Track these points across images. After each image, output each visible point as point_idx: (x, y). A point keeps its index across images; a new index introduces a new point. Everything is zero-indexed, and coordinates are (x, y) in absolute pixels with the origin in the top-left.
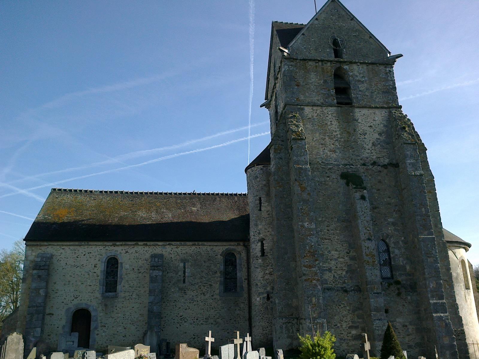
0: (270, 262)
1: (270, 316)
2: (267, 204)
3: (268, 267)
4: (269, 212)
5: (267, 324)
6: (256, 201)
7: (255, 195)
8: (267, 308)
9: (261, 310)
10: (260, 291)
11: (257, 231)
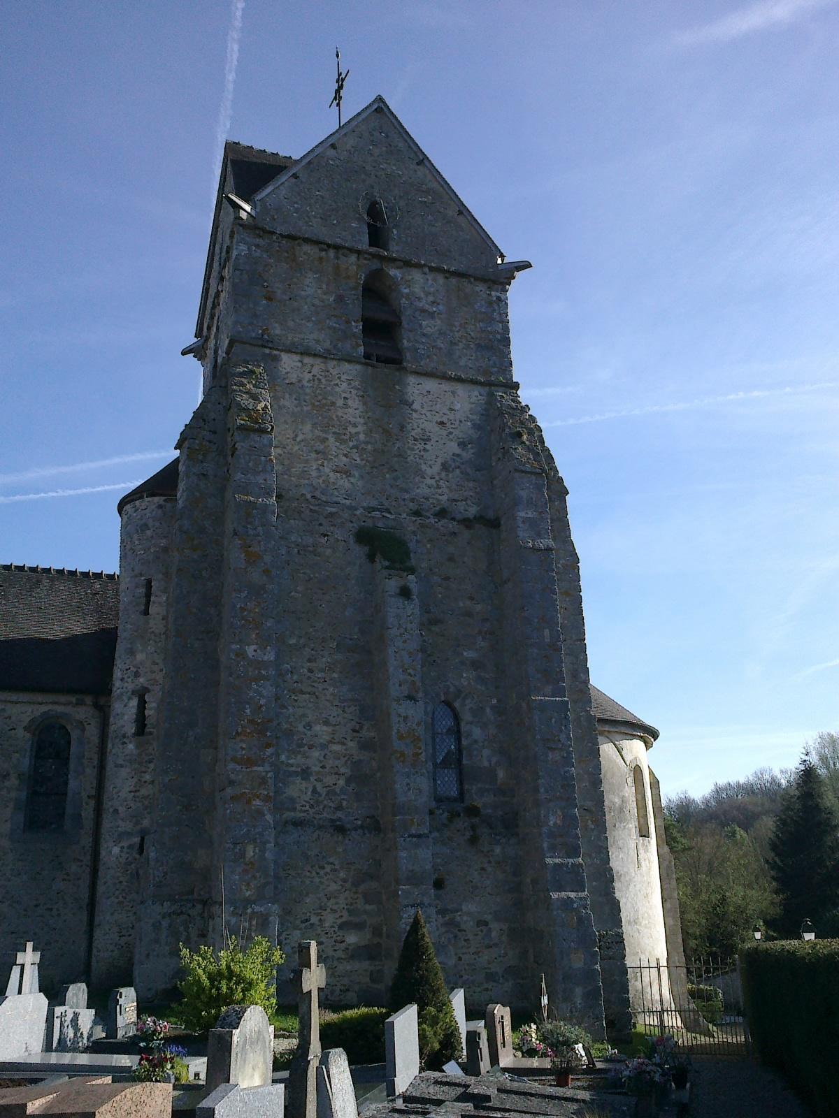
6: (137, 587)
9: (121, 879)
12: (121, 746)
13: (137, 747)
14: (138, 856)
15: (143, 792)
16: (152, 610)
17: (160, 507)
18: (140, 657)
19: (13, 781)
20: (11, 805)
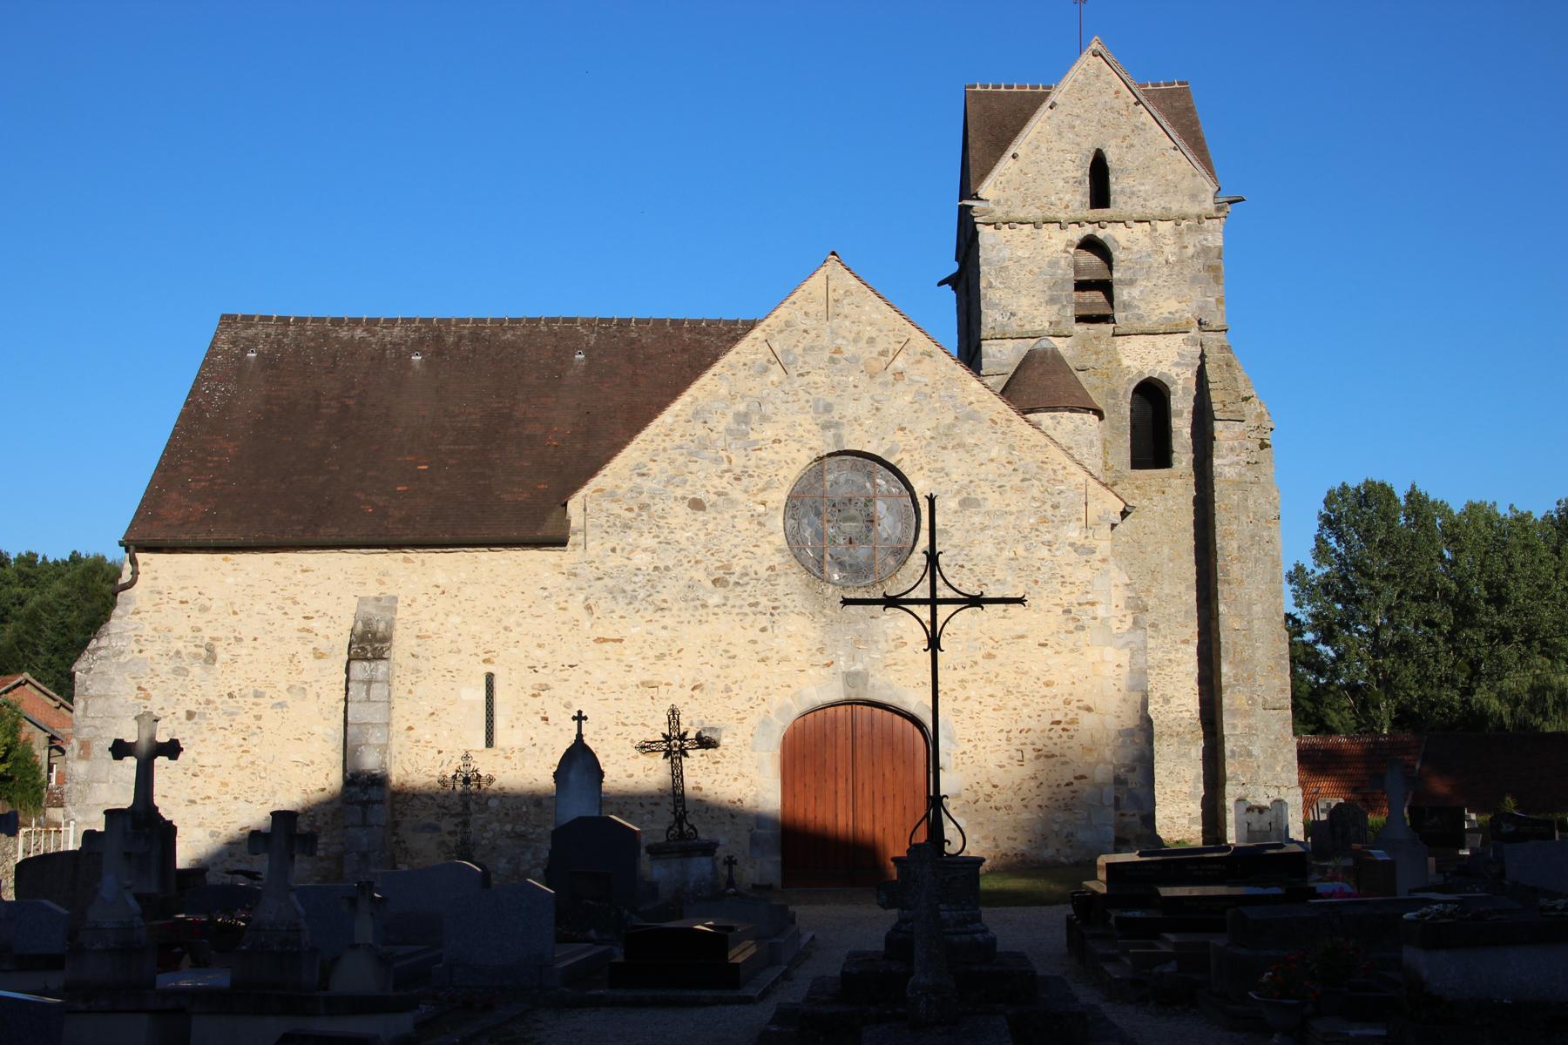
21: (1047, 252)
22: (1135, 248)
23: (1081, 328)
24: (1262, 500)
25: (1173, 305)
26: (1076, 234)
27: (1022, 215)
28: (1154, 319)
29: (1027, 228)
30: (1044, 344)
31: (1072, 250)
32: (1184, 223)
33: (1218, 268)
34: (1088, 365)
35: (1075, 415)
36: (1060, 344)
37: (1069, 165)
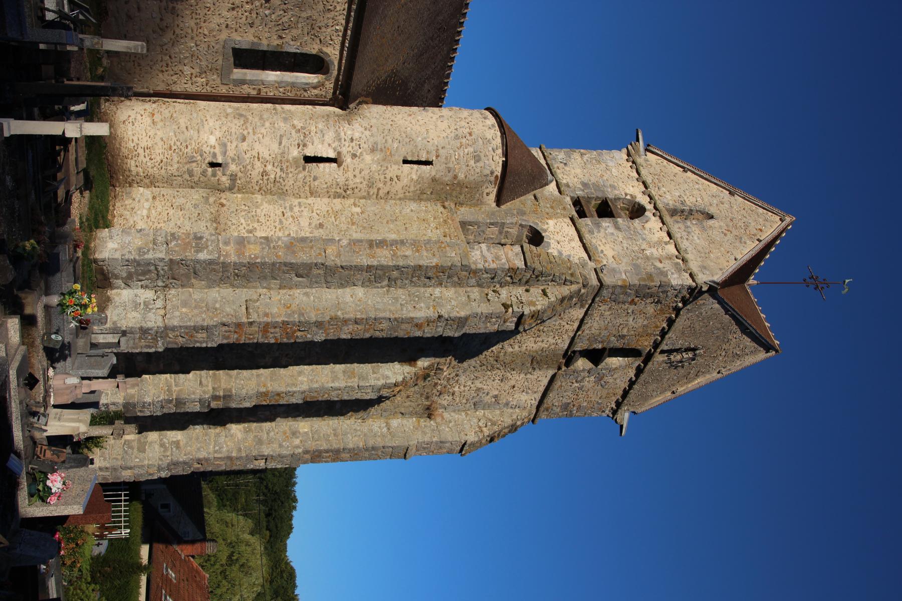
0: (290, 175)
1: (176, 166)
2: (415, 177)
3: (278, 170)
4: (395, 179)
5: (158, 159)
6: (428, 152)
7: (441, 152)
8: (191, 160)
9: (189, 147)
10: (229, 148)
11: (360, 151)
12: (296, 142)
13: (294, 158)
14: (207, 161)
15: (258, 164)
16: (407, 167)
17: (492, 173)
18: (368, 158)
19: (276, 42)
20: (256, 40)
21: (621, 184)
22: (646, 232)
23: (568, 200)
24: (453, 303)
25: (609, 253)
26: (644, 200)
27: (643, 172)
28: (594, 241)
29: (636, 175)
30: (550, 177)
31: (628, 197)
32: (680, 261)
33: (653, 281)
34: (540, 201)
35: (499, 140)
36: (552, 187)
37: (693, 200)
